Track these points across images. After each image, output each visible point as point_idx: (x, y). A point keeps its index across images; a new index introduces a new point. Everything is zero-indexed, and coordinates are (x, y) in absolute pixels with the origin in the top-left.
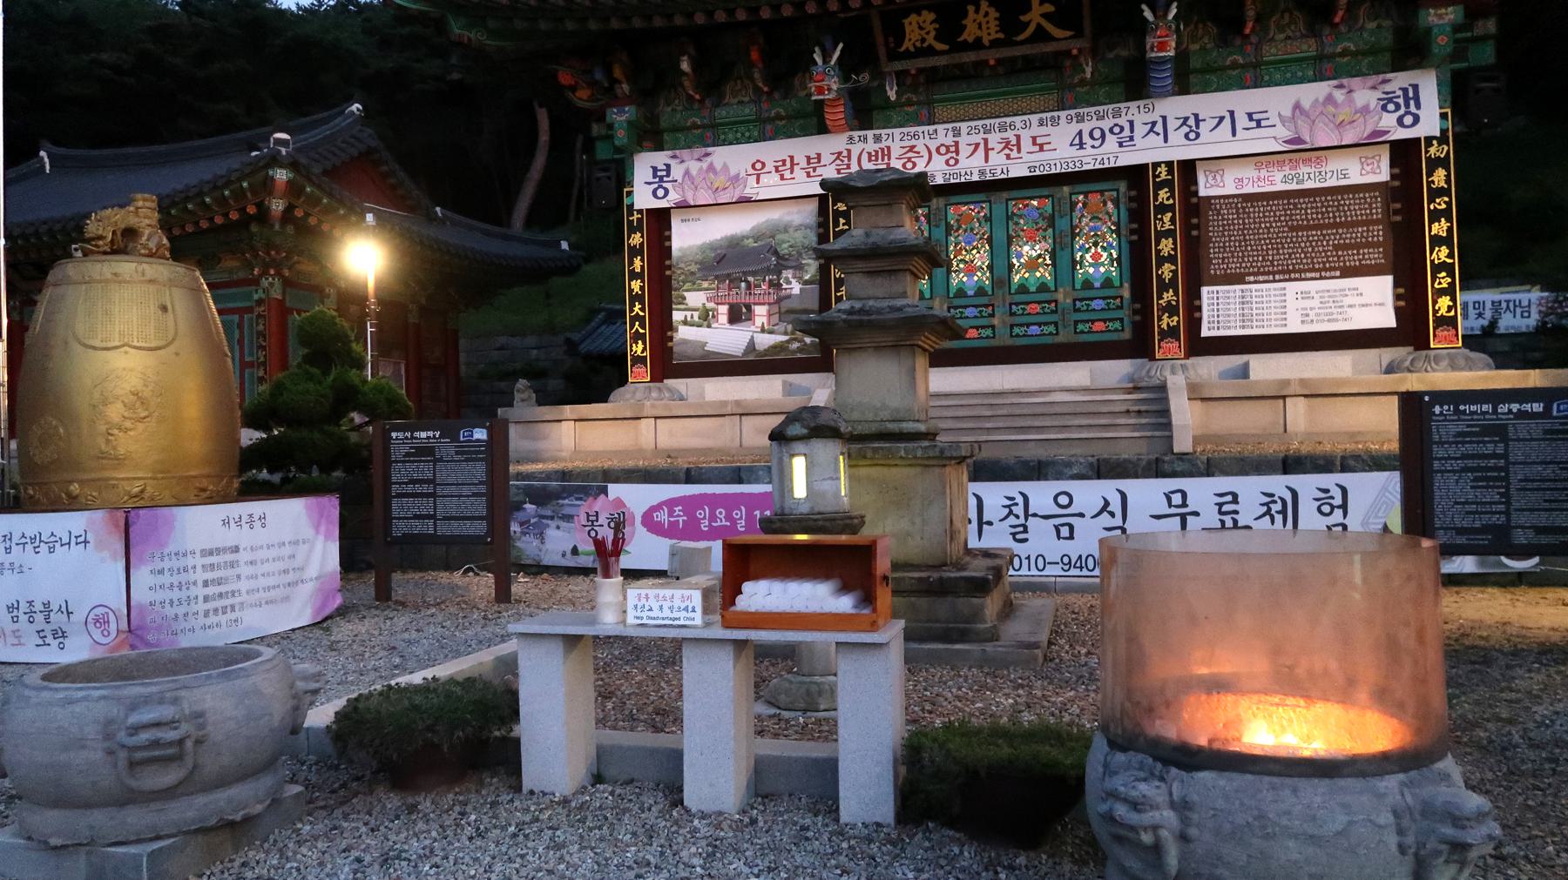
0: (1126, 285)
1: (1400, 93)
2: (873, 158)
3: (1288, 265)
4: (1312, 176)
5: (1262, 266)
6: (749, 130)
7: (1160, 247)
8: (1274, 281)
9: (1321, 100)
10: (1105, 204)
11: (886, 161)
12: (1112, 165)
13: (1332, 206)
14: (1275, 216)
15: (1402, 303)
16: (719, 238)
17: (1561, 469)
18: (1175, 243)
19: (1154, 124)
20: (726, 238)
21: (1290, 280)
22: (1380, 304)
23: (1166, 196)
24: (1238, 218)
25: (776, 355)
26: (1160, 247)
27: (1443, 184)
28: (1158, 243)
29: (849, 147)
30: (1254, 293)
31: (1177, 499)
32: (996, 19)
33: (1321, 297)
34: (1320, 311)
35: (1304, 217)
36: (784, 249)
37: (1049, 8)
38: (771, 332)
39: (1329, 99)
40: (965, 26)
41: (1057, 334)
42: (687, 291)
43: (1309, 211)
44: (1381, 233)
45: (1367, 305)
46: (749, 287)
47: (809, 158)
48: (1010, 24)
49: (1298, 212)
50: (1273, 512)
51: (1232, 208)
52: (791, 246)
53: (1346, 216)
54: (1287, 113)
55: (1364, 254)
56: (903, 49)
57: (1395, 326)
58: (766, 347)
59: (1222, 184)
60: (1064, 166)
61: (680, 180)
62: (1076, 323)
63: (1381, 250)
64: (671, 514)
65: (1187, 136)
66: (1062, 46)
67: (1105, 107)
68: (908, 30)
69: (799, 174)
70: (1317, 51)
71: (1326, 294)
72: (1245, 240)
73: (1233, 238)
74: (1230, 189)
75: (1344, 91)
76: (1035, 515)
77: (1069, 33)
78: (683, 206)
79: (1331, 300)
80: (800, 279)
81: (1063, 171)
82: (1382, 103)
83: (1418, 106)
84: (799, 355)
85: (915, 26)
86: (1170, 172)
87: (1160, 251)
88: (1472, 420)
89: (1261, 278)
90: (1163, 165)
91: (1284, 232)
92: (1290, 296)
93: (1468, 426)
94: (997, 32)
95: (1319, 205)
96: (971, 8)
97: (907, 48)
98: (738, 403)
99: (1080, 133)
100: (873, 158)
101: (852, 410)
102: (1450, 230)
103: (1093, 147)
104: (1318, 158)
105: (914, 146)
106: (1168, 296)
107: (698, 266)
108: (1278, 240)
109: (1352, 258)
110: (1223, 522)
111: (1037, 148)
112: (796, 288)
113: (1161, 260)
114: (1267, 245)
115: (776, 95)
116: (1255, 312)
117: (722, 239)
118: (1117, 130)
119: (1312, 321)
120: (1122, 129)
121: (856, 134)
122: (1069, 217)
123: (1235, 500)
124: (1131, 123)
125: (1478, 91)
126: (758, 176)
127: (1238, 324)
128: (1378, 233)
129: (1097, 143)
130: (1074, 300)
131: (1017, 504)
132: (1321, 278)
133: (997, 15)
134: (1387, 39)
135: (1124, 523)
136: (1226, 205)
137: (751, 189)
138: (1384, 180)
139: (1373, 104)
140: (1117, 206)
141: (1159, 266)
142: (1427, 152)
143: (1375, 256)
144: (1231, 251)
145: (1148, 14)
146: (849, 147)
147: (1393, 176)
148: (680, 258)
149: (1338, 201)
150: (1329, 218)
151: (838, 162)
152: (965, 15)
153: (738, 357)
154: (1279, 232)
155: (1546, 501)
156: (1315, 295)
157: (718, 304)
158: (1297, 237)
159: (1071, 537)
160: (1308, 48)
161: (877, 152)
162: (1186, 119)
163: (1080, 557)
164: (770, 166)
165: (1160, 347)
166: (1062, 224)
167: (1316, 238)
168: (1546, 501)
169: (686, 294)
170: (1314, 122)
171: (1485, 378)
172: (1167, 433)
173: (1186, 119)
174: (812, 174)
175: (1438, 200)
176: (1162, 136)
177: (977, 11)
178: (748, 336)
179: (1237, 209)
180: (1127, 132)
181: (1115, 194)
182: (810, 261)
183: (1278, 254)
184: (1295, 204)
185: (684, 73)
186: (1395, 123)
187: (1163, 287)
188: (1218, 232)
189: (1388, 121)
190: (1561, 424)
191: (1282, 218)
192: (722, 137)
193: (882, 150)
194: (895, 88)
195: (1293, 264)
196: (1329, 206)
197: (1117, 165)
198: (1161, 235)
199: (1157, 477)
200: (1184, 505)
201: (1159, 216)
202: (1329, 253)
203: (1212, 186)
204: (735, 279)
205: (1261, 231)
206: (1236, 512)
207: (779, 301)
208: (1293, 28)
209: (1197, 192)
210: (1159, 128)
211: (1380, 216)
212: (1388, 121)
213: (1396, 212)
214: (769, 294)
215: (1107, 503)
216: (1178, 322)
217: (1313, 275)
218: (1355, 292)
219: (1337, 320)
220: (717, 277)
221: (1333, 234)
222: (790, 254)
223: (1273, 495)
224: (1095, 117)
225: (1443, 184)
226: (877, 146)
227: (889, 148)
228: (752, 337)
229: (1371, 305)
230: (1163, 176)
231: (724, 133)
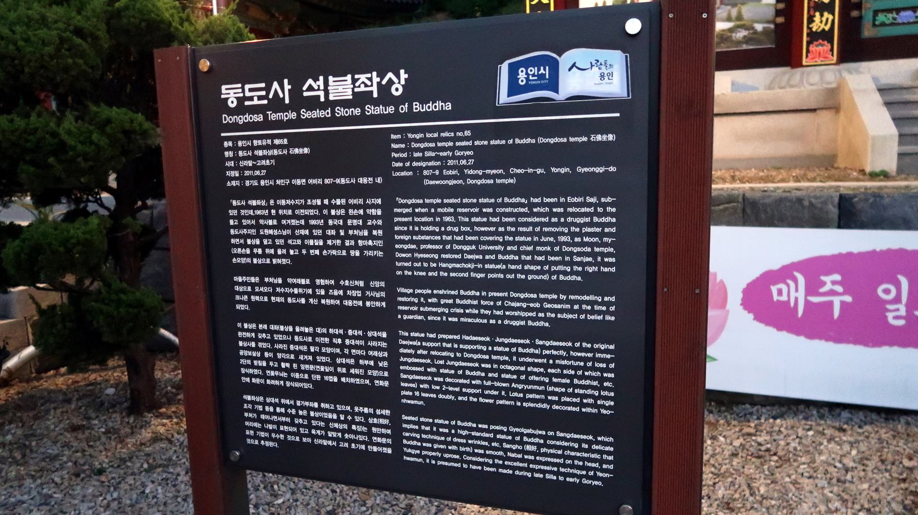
64: (813, 288)
84: (745, 47)
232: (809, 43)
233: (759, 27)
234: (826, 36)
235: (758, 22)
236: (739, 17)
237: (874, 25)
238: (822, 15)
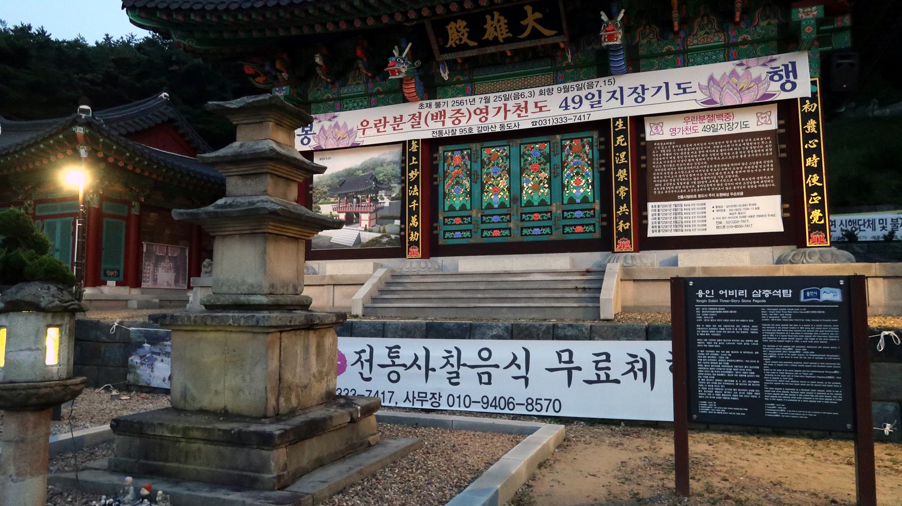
0: (597, 201)
1: (783, 68)
2: (435, 118)
3: (707, 187)
4: (723, 126)
5: (689, 188)
6: (362, 101)
7: (618, 175)
8: (697, 199)
9: (728, 74)
10: (584, 146)
11: (442, 119)
12: (586, 120)
13: (738, 147)
14: (698, 154)
15: (788, 215)
16: (341, 170)
17: (809, 350)
18: (628, 172)
19: (615, 92)
20: (346, 170)
21: (709, 198)
22: (772, 215)
23: (622, 140)
24: (673, 156)
25: (373, 245)
26: (618, 175)
27: (814, 130)
28: (616, 173)
29: (420, 110)
30: (683, 207)
31: (565, 356)
32: (505, 24)
33: (730, 210)
34: (731, 220)
35: (718, 154)
36: (380, 177)
37: (538, 15)
38: (370, 231)
39: (734, 73)
40: (486, 29)
41: (551, 234)
42: (321, 204)
43: (721, 150)
44: (772, 165)
45: (762, 216)
46: (358, 202)
47: (395, 118)
48: (515, 28)
49: (714, 151)
50: (636, 370)
51: (668, 149)
52: (384, 175)
53: (747, 154)
54: (706, 84)
55: (760, 180)
56: (448, 46)
57: (783, 230)
58: (367, 241)
59: (661, 133)
60: (555, 121)
61: (317, 133)
62: (564, 226)
63: (772, 177)
65: (636, 100)
66: (550, 41)
67: (583, 82)
68: (450, 32)
69: (389, 128)
70: (725, 41)
71: (734, 208)
72: (677, 171)
73: (669, 169)
74: (666, 135)
75: (744, 67)
76: (465, 365)
77: (553, 33)
78: (319, 150)
79: (737, 212)
80: (389, 196)
81: (554, 124)
82: (770, 75)
83: (795, 77)
84: (387, 246)
85: (454, 30)
86: (625, 124)
87: (618, 178)
88: (730, 303)
89: (688, 197)
90: (620, 120)
91: (704, 165)
92: (709, 210)
93: (727, 309)
94: (507, 33)
95: (728, 146)
96: (488, 17)
97: (451, 45)
98: (332, 277)
99: (566, 99)
100: (435, 118)
101: (222, 285)
102: (819, 163)
103: (574, 108)
104: (727, 114)
105: (460, 110)
106: (624, 208)
107: (328, 188)
109: (752, 183)
110: (598, 376)
111: (538, 110)
112: (387, 202)
113: (619, 184)
114: (692, 173)
115: (378, 78)
116: (684, 220)
117: (343, 171)
118: (590, 96)
119: (724, 226)
120: (593, 96)
121: (425, 102)
122: (560, 155)
123: (608, 359)
124: (600, 92)
125: (839, 65)
126: (364, 130)
127: (673, 228)
128: (770, 165)
129: (577, 106)
130: (563, 211)
131: (452, 356)
132: (730, 197)
133: (506, 21)
134: (773, 32)
135: (527, 374)
136: (665, 146)
137: (360, 139)
138: (774, 129)
140: (591, 148)
141: (617, 188)
142: (802, 108)
143: (768, 182)
144: (667, 178)
145: (604, 17)
146: (420, 110)
147: (780, 126)
148: (318, 183)
149: (742, 143)
150: (735, 155)
151: (413, 120)
152: (486, 23)
153: (350, 247)
154: (701, 165)
155: (795, 379)
156: (726, 208)
157: (339, 212)
158: (713, 168)
159: (489, 383)
160: (718, 39)
161: (437, 113)
162: (636, 88)
163: (495, 398)
164: (371, 124)
165: (617, 244)
166: (556, 160)
167: (726, 169)
168: (795, 379)
169: (320, 206)
170: (722, 89)
171: (836, 268)
172: (597, 305)
173: (636, 88)
174: (396, 128)
175: (810, 142)
176: (619, 100)
177: (492, 19)
178: (357, 233)
179: (672, 149)
180: (596, 98)
181: (590, 139)
182: (396, 185)
183: (700, 180)
184: (712, 146)
185: (317, 65)
186: (779, 89)
187: (620, 202)
188: (658, 165)
189: (774, 87)
190: (808, 309)
191: (703, 156)
192: (345, 106)
193: (440, 112)
194: (447, 72)
195: (710, 187)
196: (735, 147)
197: (589, 120)
198: (619, 167)
199: (553, 339)
200: (571, 361)
201: (617, 154)
202: (736, 180)
203: (655, 134)
204: (351, 196)
205: (688, 164)
206: (608, 368)
207: (376, 210)
208: (710, 26)
209: (645, 138)
210: (618, 95)
211: (771, 154)
212: (774, 87)
213: (782, 151)
214: (370, 206)
215: (515, 358)
216: (630, 226)
217: (724, 194)
218: (754, 207)
219: (741, 226)
220: (339, 195)
221: (738, 166)
222: (384, 181)
223: (635, 356)
224: (576, 88)
225: (814, 130)
226: (437, 110)
227: (444, 111)
228: (359, 234)
229: (765, 216)
230: (620, 127)
231: (347, 104)
232: (409, 247)
233: (393, 237)
234: (416, 243)
235: (393, 234)
236: (384, 231)
237: (444, 238)
238: (414, 233)
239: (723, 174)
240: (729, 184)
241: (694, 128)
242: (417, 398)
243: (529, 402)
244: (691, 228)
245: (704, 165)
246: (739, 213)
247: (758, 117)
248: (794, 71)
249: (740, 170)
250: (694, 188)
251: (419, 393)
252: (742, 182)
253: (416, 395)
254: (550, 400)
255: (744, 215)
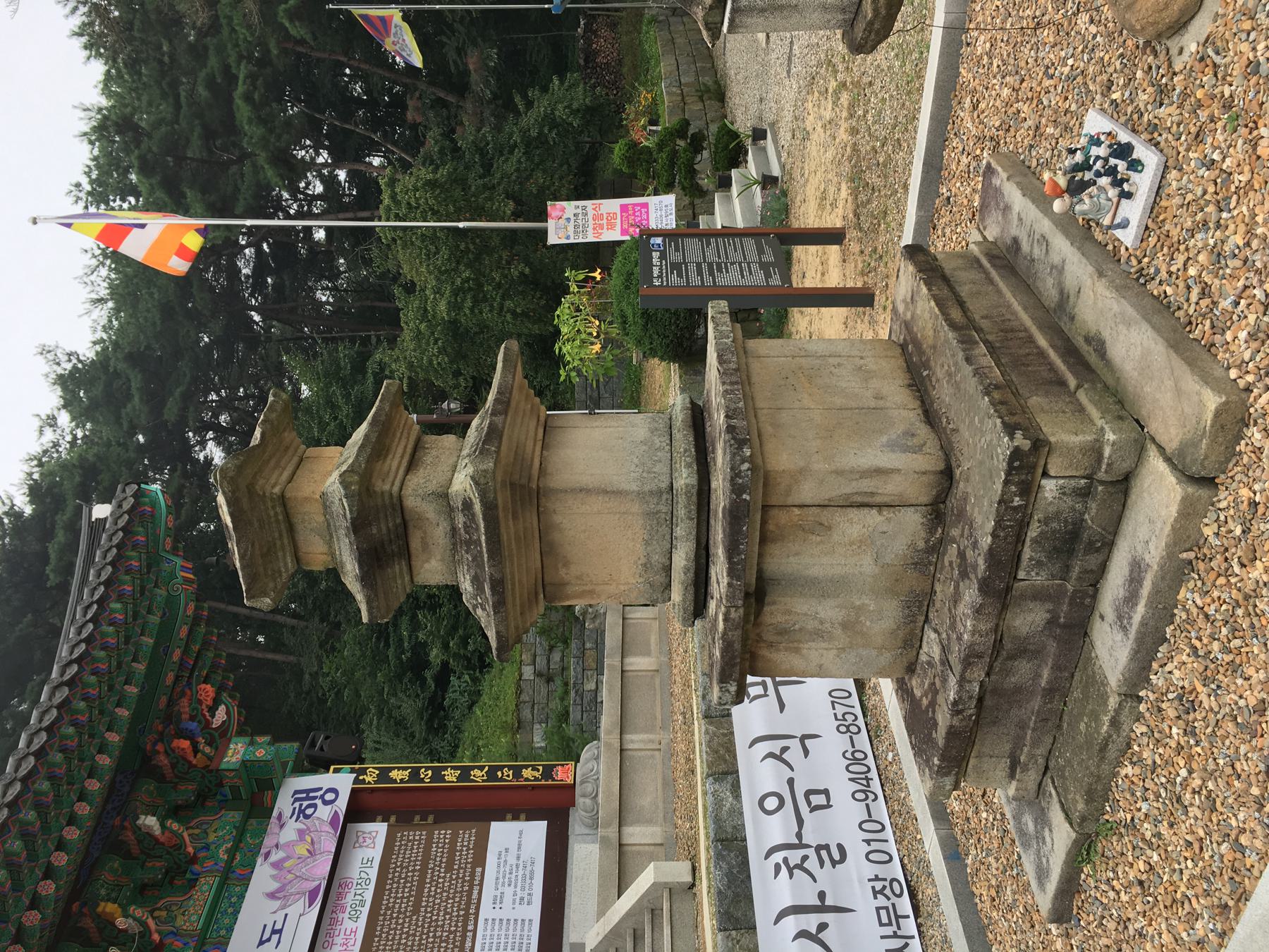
1: (297, 805)
3: (458, 916)
8: (475, 931)
9: (274, 872)
21: (477, 914)
27: (407, 773)
33: (503, 885)
35: (405, 900)
39: (276, 865)
49: (397, 906)
54: (277, 904)
71: (501, 880)
76: (799, 836)
79: (508, 876)
83: (320, 789)
91: (417, 920)
104: (340, 885)
108: (426, 926)
109: (465, 855)
119: (529, 894)
125: (321, 749)
128: (442, 835)
131: (786, 860)
132: (481, 885)
135: (796, 737)
139: (299, 825)
142: (369, 783)
143: (467, 837)
150: (413, 876)
154: (416, 924)
155: (736, 251)
156: (500, 891)
159: (826, 792)
160: (207, 887)
163: (850, 779)
167: (433, 889)
168: (736, 251)
171: (610, 691)
172: (666, 895)
175: (422, 776)
183: (443, 926)
184: (387, 908)
189: (324, 812)
191: (401, 921)
195: (458, 911)
196: (400, 876)
212: (324, 812)
215: (771, 755)
217: (475, 892)
218: (503, 853)
219: (532, 872)
221: (432, 873)
225: (407, 773)
239: (441, 893)
240: (459, 885)
241: (348, 933)
242: (894, 928)
243: (845, 727)
244: (525, 941)
245: (417, 920)
246: (511, 873)
247: (361, 846)
248: (308, 791)
249: (439, 871)
250: (456, 936)
251: (881, 924)
252: (460, 868)
253: (889, 931)
254: (833, 703)
255: (514, 867)
